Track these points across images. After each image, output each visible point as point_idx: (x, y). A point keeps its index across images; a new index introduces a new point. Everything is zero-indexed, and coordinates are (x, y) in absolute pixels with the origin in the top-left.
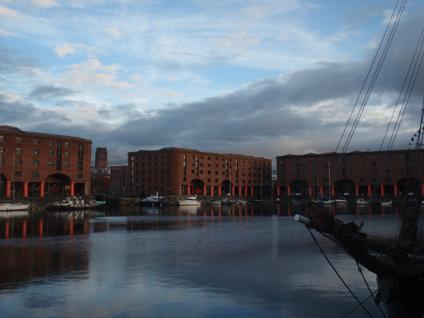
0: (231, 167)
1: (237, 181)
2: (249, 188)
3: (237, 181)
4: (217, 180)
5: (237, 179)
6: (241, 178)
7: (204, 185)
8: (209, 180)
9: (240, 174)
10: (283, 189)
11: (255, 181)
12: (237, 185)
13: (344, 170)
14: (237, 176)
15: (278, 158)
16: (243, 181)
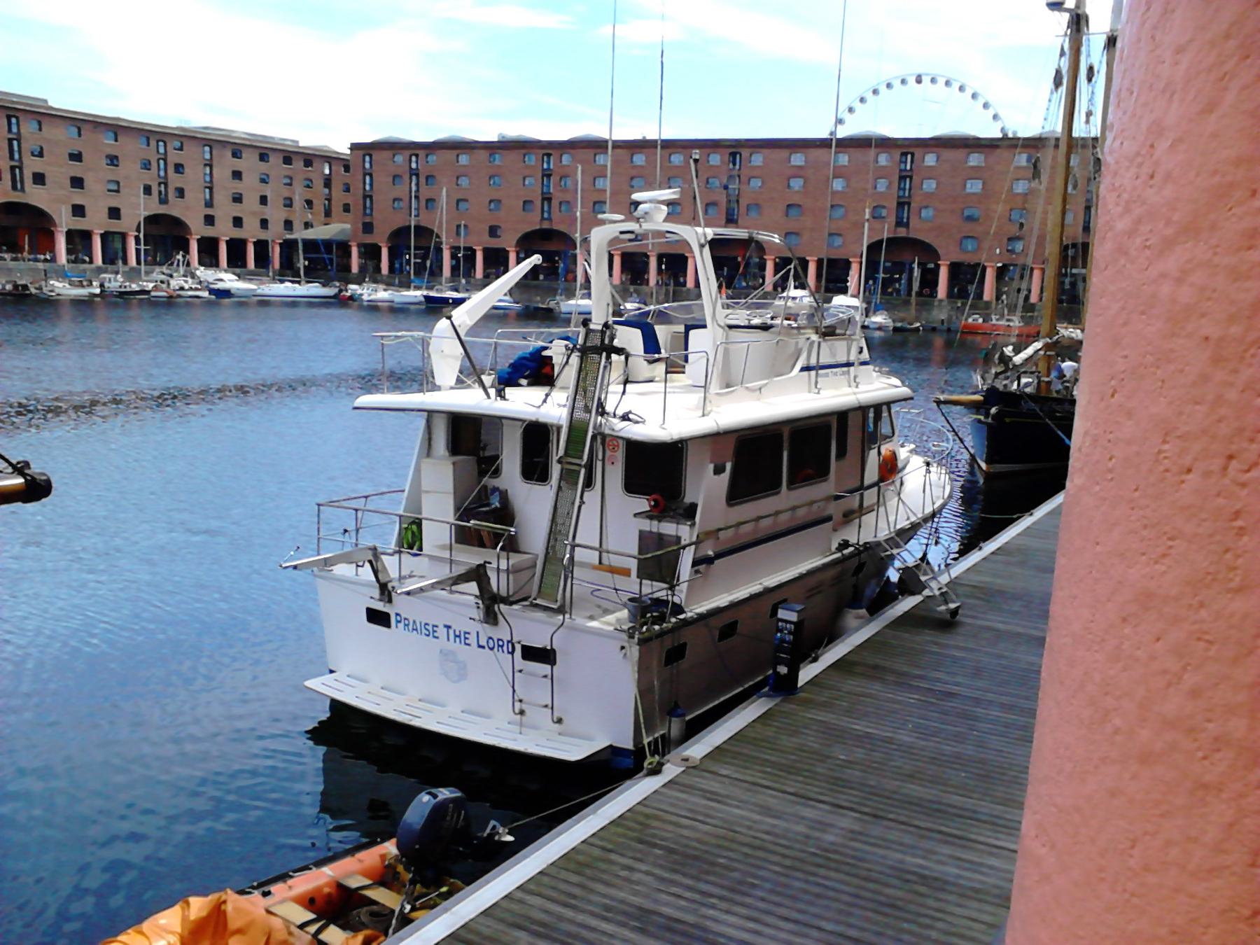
0: (179, 168)
1: (210, 220)
2: (262, 246)
3: (210, 220)
4: (114, 213)
5: (209, 212)
6: (224, 211)
7: (55, 225)
8: (79, 211)
9: (222, 198)
10: (371, 253)
11: (288, 225)
12: (209, 232)
13: (547, 198)
14: (209, 204)
15: (355, 147)
16: (238, 222)
